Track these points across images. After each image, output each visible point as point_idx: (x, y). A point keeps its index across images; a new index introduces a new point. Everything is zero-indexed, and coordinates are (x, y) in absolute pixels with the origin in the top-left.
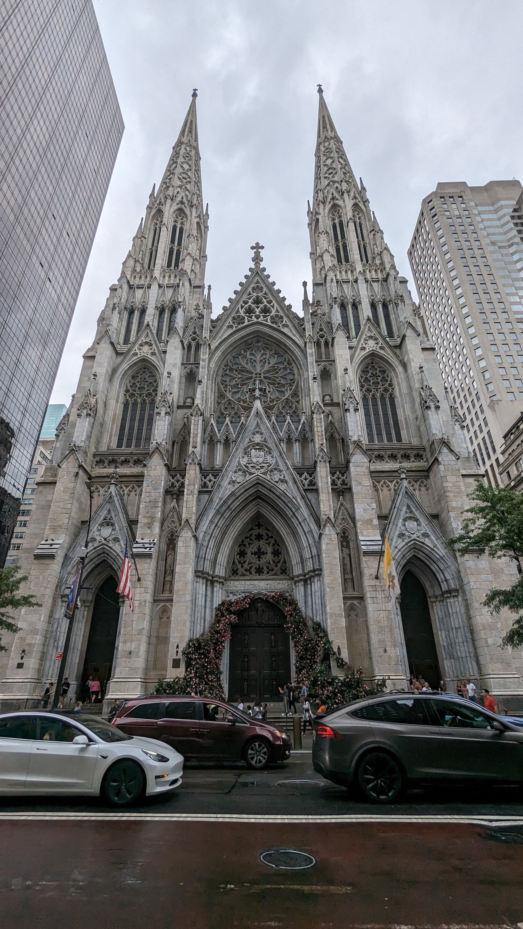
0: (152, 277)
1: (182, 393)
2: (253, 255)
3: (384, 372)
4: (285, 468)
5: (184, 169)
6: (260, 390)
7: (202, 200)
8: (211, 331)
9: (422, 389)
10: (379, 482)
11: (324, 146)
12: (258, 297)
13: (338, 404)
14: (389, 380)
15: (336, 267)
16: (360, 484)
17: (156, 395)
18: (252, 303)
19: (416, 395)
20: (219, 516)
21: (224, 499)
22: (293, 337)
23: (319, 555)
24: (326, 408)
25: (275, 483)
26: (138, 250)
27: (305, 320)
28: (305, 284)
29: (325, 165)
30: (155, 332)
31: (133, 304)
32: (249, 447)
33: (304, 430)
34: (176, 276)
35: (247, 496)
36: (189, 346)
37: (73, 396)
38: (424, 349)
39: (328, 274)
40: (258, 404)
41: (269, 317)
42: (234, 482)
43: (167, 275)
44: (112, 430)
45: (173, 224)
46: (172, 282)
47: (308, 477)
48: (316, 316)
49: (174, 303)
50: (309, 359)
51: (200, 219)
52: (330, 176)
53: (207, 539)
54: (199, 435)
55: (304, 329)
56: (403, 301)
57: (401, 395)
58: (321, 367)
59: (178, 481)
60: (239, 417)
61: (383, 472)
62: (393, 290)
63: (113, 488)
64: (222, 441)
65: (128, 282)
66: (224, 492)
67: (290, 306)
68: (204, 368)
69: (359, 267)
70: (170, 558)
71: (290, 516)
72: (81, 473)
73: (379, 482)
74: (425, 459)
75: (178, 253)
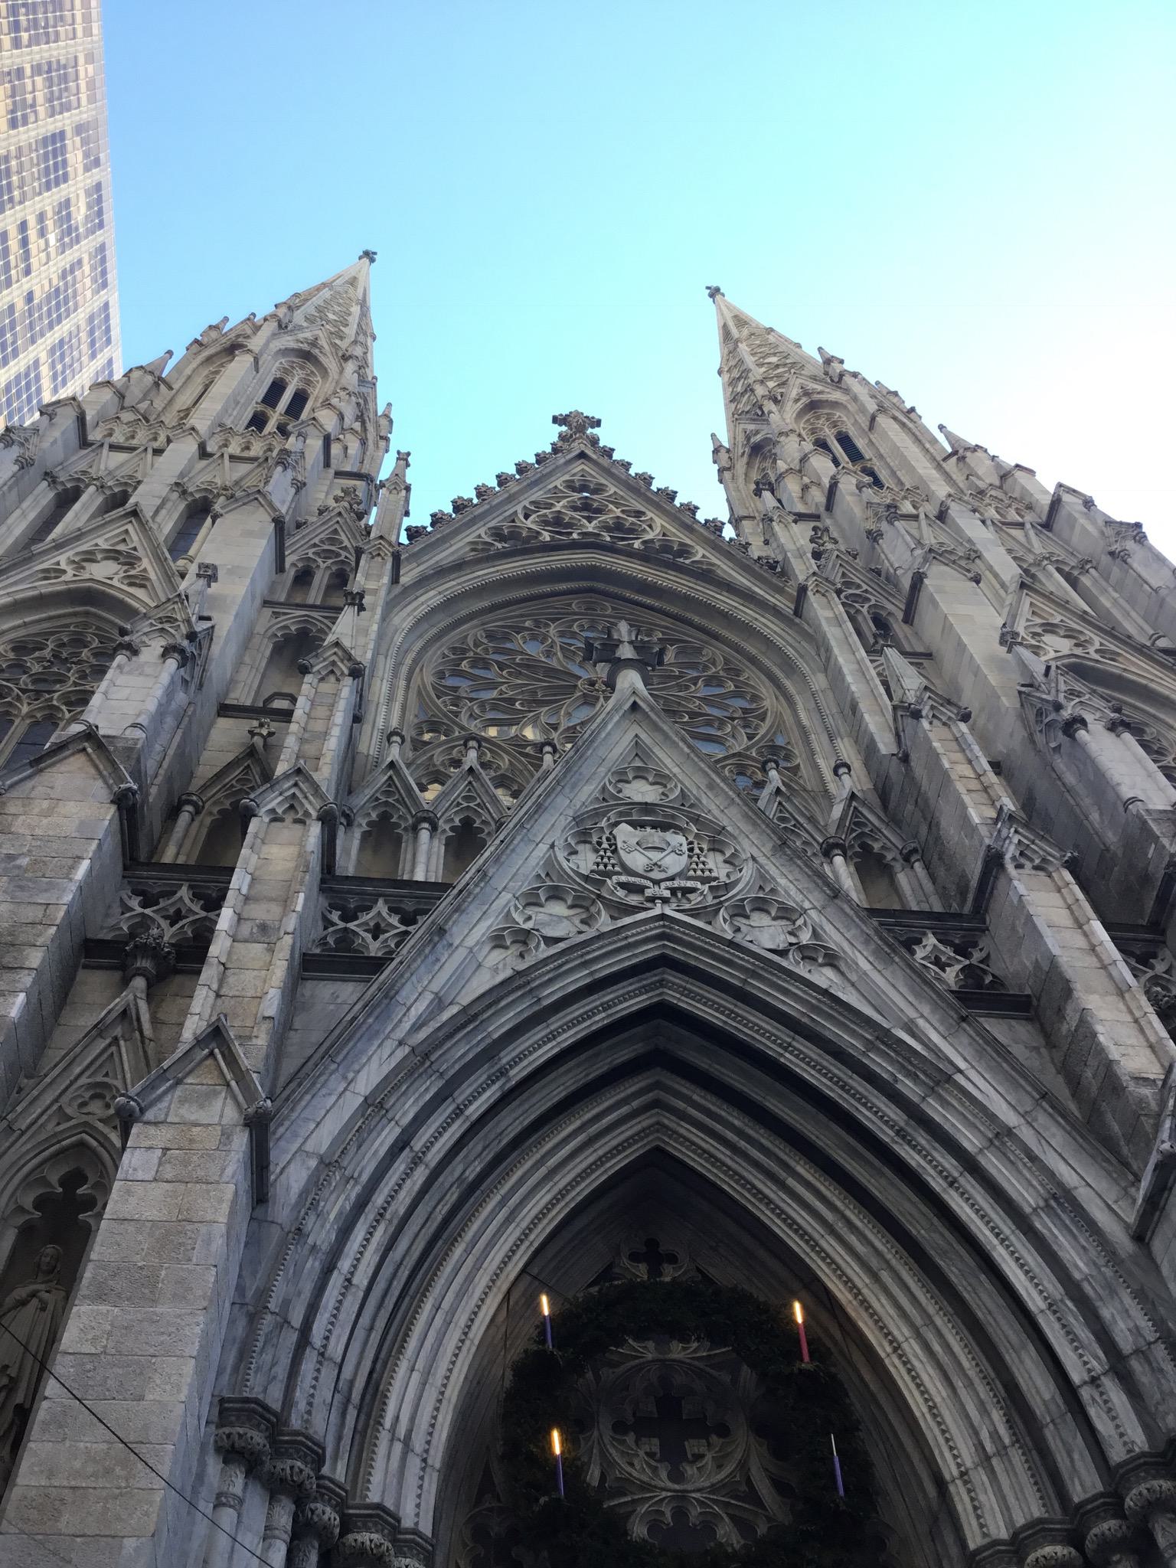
20: (428, 1088)
32: (598, 814)
35: (600, 1020)
42: (523, 937)
53: (337, 1205)
64: (447, 827)
66: (460, 978)
71: (886, 1135)
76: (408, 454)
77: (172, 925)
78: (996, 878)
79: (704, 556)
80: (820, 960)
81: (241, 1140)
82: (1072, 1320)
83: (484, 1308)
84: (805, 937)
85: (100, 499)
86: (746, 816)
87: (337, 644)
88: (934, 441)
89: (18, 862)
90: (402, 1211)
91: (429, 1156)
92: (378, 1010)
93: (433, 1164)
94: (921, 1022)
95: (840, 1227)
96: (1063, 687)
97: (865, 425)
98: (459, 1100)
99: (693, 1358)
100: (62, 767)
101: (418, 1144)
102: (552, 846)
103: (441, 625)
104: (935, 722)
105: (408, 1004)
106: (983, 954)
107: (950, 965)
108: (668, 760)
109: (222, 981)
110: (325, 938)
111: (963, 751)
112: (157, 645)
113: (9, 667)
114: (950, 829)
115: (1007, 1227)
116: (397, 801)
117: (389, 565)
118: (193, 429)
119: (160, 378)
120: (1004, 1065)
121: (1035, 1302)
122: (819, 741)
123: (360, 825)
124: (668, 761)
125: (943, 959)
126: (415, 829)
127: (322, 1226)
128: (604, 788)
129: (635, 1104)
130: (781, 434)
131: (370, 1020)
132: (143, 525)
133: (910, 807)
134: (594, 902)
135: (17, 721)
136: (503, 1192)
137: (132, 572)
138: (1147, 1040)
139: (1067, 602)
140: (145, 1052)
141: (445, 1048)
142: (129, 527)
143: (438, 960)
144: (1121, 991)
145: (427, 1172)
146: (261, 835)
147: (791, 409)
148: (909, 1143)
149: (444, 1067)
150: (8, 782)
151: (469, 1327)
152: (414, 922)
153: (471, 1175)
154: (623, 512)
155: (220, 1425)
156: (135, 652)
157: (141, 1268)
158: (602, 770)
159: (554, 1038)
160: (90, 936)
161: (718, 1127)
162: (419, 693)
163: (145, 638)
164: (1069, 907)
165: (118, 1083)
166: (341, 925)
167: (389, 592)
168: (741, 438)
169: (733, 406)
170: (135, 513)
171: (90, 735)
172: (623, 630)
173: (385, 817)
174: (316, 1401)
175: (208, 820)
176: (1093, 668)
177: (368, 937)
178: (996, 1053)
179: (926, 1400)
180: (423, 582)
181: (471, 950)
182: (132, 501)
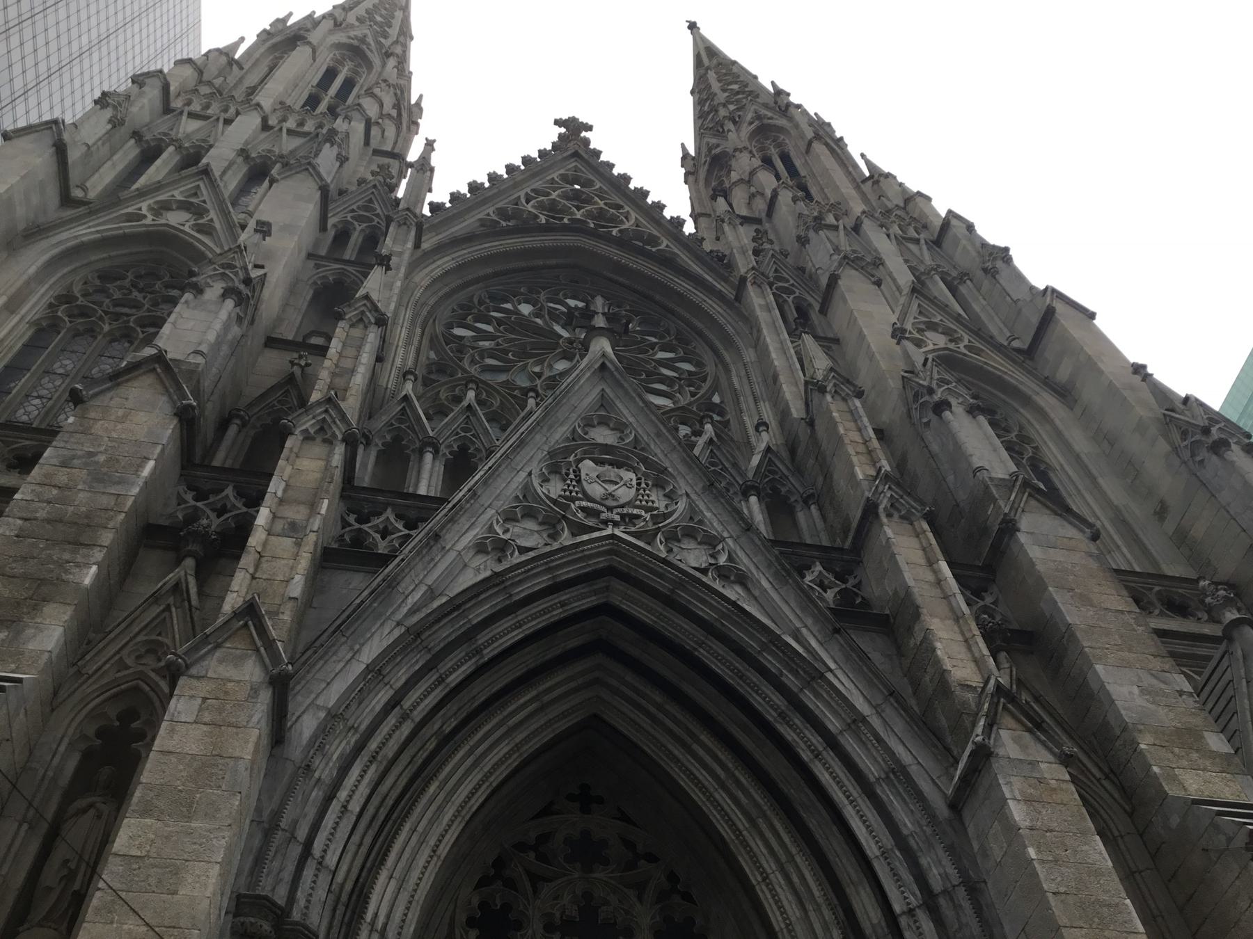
20: (417, 661)
23: (974, 889)
25: (698, 574)
32: (567, 451)
35: (557, 614)
42: (502, 547)
53: (338, 748)
66: (451, 574)
70: (77, 832)
71: (771, 716)
76: (434, 141)
77: (219, 517)
78: (871, 523)
79: (667, 246)
80: (732, 578)
81: (265, 696)
82: (897, 864)
83: (450, 832)
84: (722, 560)
85: (177, 158)
86: (683, 460)
87: (367, 297)
88: (856, 166)
89: (96, 459)
90: (390, 755)
91: (415, 713)
92: (382, 597)
93: (417, 720)
94: (804, 631)
95: (730, 784)
96: (936, 376)
97: (803, 149)
98: (442, 671)
99: (610, 878)
100: (136, 383)
101: (407, 704)
102: (530, 474)
103: (453, 285)
104: (837, 397)
105: (407, 593)
106: (857, 581)
107: (830, 588)
108: (626, 412)
109: (257, 567)
110: (342, 536)
111: (855, 421)
112: (217, 288)
113: (96, 291)
114: (840, 483)
115: (855, 792)
116: (408, 427)
117: (413, 233)
118: (258, 105)
119: (233, 59)
120: (865, 668)
121: (871, 850)
122: (747, 403)
123: (377, 445)
124: (625, 412)
125: (826, 582)
126: (421, 453)
127: (327, 764)
128: (574, 430)
130: (735, 150)
131: (375, 605)
132: (213, 184)
133: (811, 462)
134: (559, 521)
135: (100, 337)
136: (471, 743)
137: (200, 222)
138: (973, 656)
139: (947, 306)
140: (192, 618)
141: (434, 629)
143: (433, 559)
144: (958, 618)
145: (412, 726)
146: (295, 450)
147: (746, 130)
148: (787, 723)
149: (432, 644)
150: (91, 392)
151: (437, 846)
152: (415, 527)
153: (447, 729)
154: (605, 204)
155: (235, 916)
157: (180, 791)
158: (574, 416)
159: (520, 626)
160: (151, 521)
162: (431, 340)
163: (209, 280)
164: (924, 550)
165: (168, 641)
166: (357, 526)
167: (412, 255)
168: (704, 150)
169: (701, 121)
170: (206, 172)
171: (160, 358)
172: (599, 304)
173: (397, 439)
174: (313, 900)
175: (252, 433)
177: (377, 536)
178: (859, 661)
179: (784, 919)
180: (440, 249)
181: (460, 553)
182: (204, 161)
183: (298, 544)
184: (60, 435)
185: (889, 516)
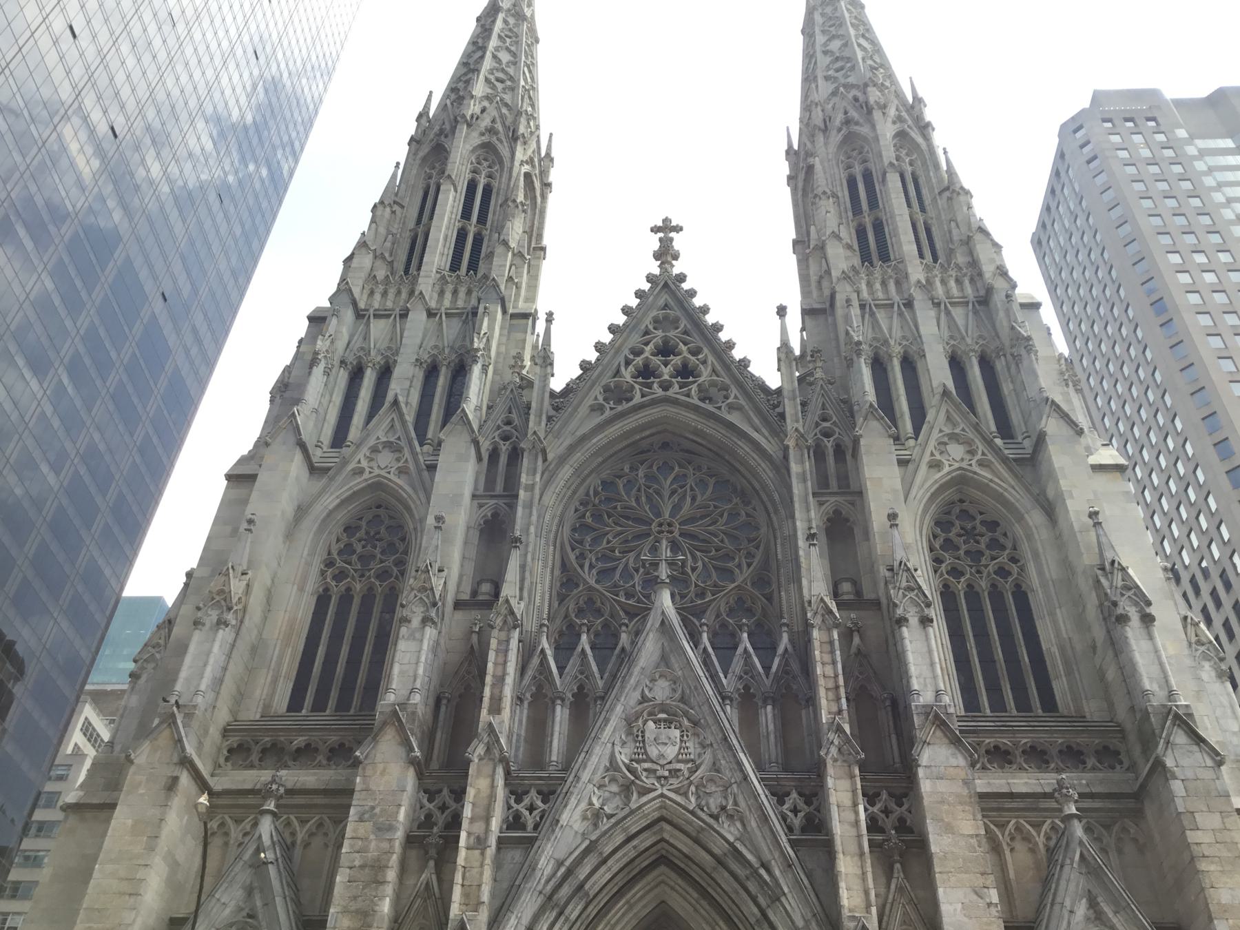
0: (411, 293)
1: (470, 568)
2: (656, 245)
3: (993, 525)
4: (738, 776)
5: (499, 61)
6: (671, 564)
7: (538, 127)
8: (549, 419)
9: (1103, 569)
10: (1002, 826)
11: (822, 15)
12: (666, 341)
13: (876, 604)
14: (1009, 545)
15: (857, 273)
16: (949, 829)
17: (402, 573)
18: (653, 354)
19: (1084, 585)
20: (554, 914)
21: (567, 863)
22: (755, 435)
24: (845, 613)
26: (382, 230)
27: (785, 393)
28: (782, 311)
29: (825, 53)
30: (410, 418)
31: (361, 354)
32: (638, 716)
33: (787, 673)
34: (469, 292)
35: (633, 854)
36: (494, 454)
37: (189, 575)
38: (1099, 468)
39: (837, 289)
40: (666, 600)
41: (694, 387)
43: (449, 289)
44: (279, 664)
45: (468, 176)
46: (460, 303)
47: (801, 804)
48: (811, 384)
49: (462, 351)
50: (797, 489)
51: (533, 166)
52: (839, 74)
54: (509, 680)
55: (782, 416)
56: (1029, 348)
57: (1044, 585)
58: (828, 507)
59: (443, 808)
60: (616, 636)
61: (1011, 796)
62: (1005, 323)
63: (266, 827)
64: (569, 695)
65: (354, 303)
67: (744, 363)
68: (529, 505)
69: (916, 272)
71: (753, 920)
72: (185, 779)
73: (1002, 826)
74: (1126, 764)
75: (478, 240)
94: (773, 862)
102: (613, 744)
109: (463, 879)
124: (676, 666)
126: (553, 702)
129: (652, 884)
142: (394, 415)
156: (409, 621)
161: (688, 897)
176: (972, 478)
177: (527, 813)
180: (562, 460)
183: (483, 854)
184: (356, 796)
185: (835, 760)
